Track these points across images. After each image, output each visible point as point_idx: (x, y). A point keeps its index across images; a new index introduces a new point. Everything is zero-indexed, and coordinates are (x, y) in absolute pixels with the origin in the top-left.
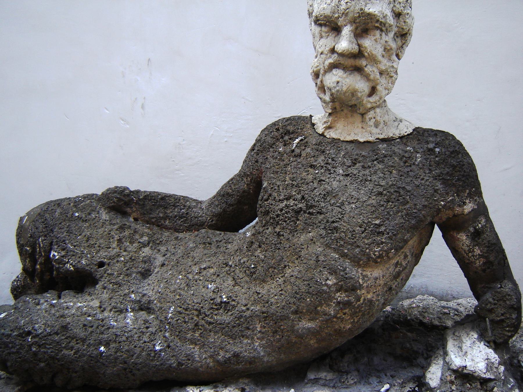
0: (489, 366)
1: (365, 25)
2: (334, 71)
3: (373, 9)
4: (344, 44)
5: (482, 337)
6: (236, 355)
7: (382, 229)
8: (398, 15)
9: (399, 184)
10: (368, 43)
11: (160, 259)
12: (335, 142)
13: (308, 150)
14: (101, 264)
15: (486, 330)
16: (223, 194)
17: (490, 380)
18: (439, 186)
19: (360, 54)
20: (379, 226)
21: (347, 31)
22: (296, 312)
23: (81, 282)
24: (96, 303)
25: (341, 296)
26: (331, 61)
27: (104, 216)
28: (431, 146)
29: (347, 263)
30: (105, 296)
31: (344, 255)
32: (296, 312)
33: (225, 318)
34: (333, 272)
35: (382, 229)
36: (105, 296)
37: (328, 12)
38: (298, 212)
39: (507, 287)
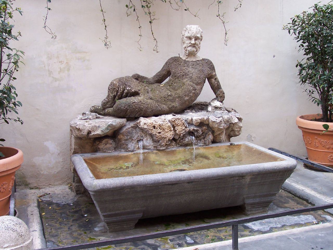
1: (197, 38)
2: (190, 47)
4: (193, 42)
5: (218, 101)
6: (173, 106)
7: (200, 77)
8: (201, 36)
9: (202, 69)
10: (197, 42)
12: (188, 61)
13: (183, 63)
15: (219, 99)
16: (157, 75)
17: (221, 108)
18: (209, 69)
19: (195, 44)
20: (200, 77)
21: (193, 39)
22: (185, 96)
23: (136, 94)
25: (193, 91)
26: (189, 45)
27: (135, 80)
28: (207, 62)
29: (194, 85)
31: (194, 83)
32: (185, 96)
33: (170, 98)
34: (192, 86)
35: (200, 77)
37: (190, 36)
38: (183, 75)
39: (221, 90)
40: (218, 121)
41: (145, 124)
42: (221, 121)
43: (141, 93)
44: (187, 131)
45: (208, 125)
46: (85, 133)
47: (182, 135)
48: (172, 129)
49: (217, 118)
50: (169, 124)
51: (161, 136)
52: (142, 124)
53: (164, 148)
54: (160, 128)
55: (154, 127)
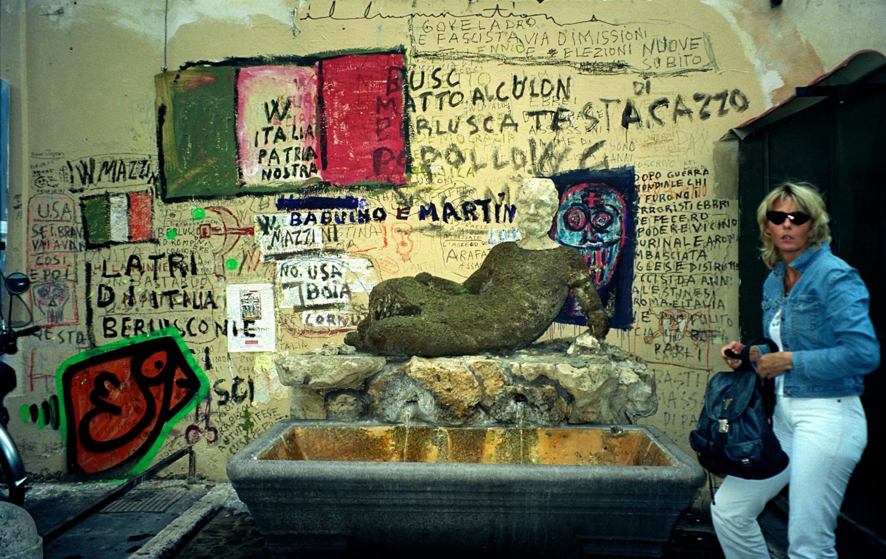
0: (593, 343)
3: (543, 198)
5: (591, 334)
10: (540, 211)
11: (447, 304)
14: (421, 304)
19: (537, 215)
21: (533, 206)
24: (423, 318)
25: (530, 311)
30: (426, 316)
33: (481, 322)
34: (527, 300)
36: (426, 316)
38: (512, 278)
40: (575, 375)
41: (419, 369)
42: (582, 376)
43: (425, 310)
44: (509, 391)
45: (556, 383)
46: (300, 377)
47: (497, 398)
48: (476, 384)
49: (575, 370)
50: (470, 373)
51: (451, 396)
52: (413, 369)
53: (458, 423)
54: (450, 380)
55: (438, 378)
